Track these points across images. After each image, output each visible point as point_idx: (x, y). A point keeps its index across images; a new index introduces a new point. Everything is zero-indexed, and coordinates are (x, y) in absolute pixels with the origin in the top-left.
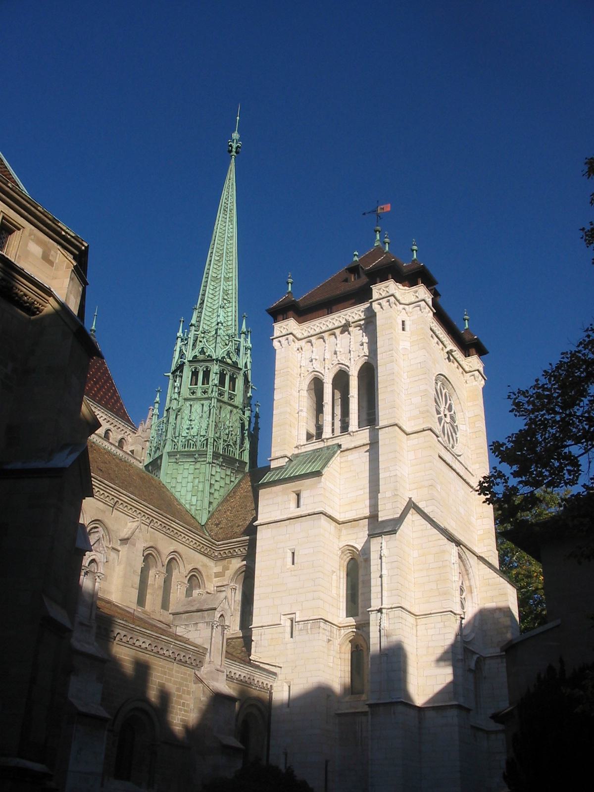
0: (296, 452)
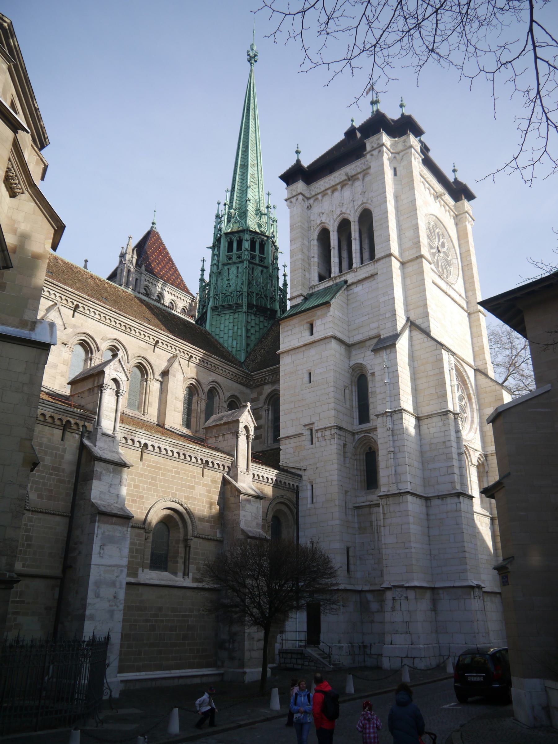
0: (311, 292)
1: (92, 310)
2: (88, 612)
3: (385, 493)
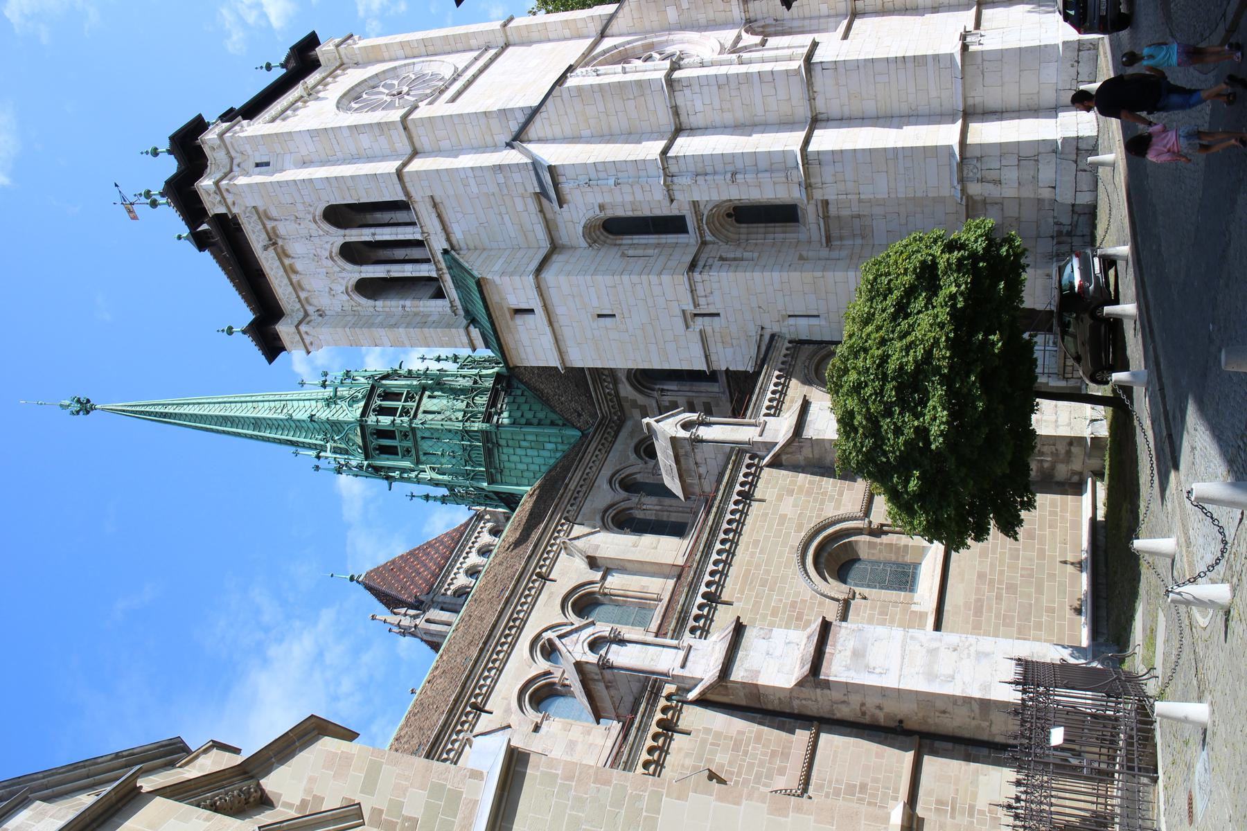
0: (461, 312)
1: (482, 682)
2: (977, 694)
3: (803, 190)
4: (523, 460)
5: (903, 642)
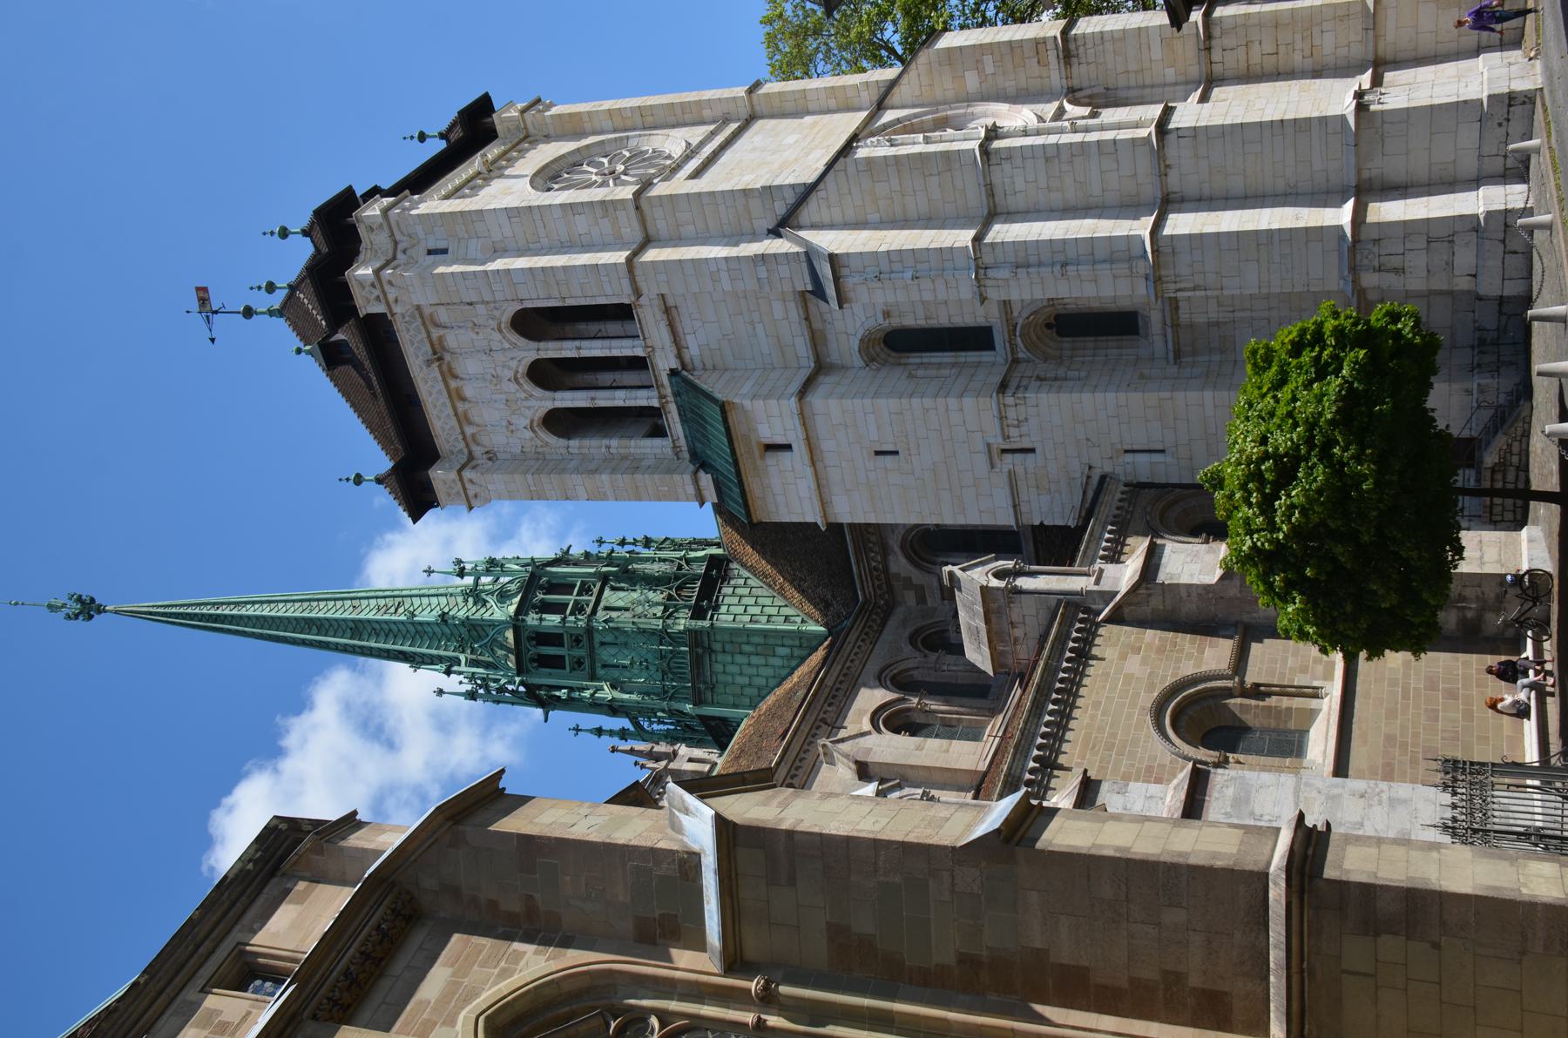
0: (686, 455)
3: (1151, 284)
4: (744, 672)
5: (1295, 788)
